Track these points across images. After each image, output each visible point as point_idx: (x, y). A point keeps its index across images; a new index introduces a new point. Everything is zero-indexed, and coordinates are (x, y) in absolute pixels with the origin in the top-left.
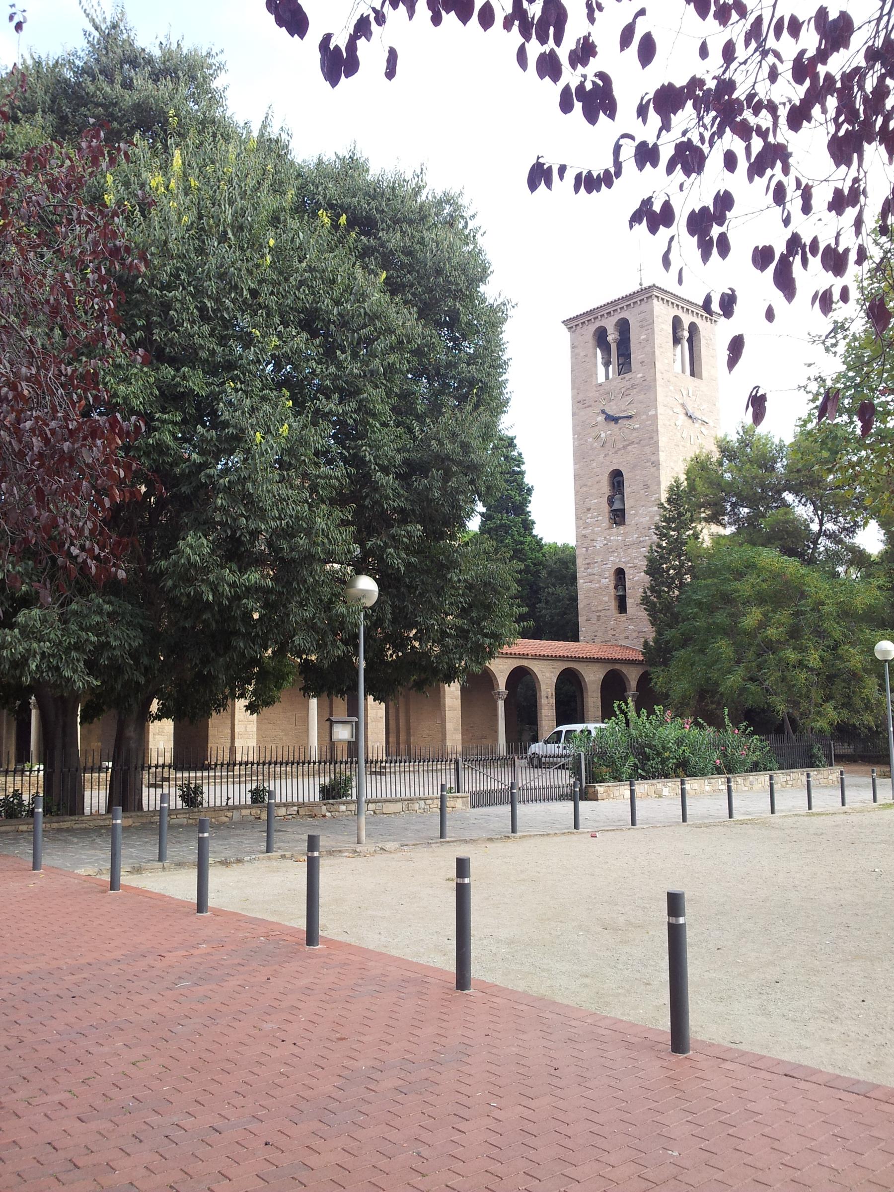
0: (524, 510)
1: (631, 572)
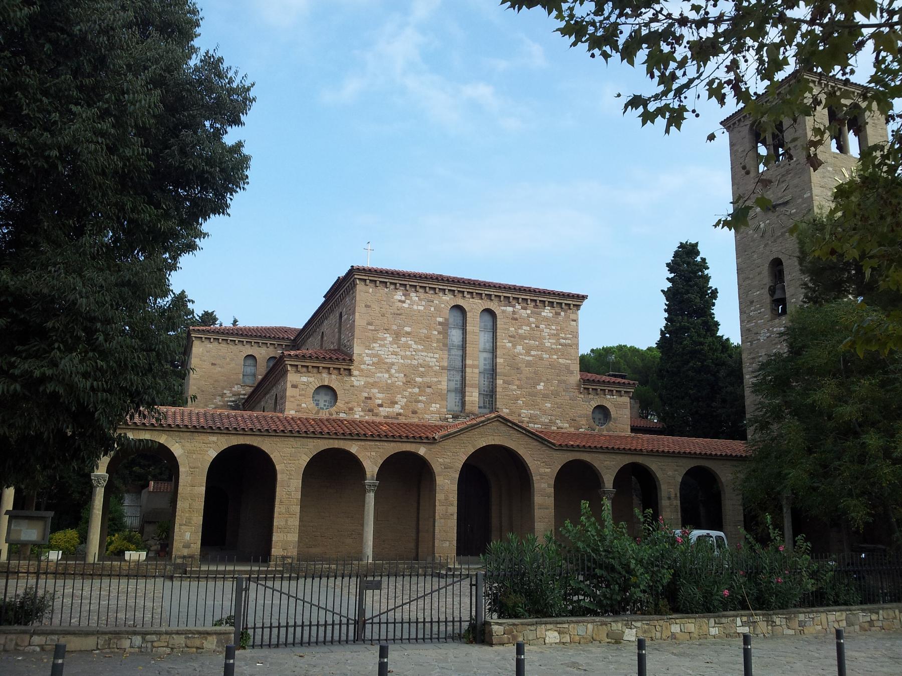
0: (705, 312)
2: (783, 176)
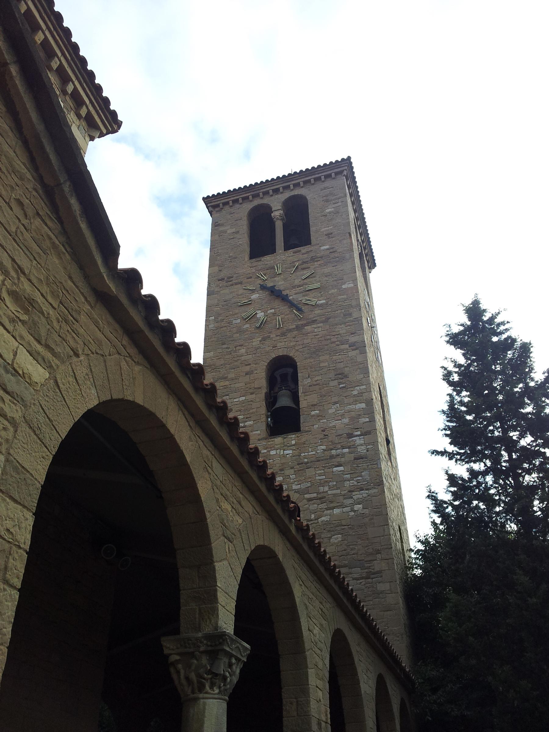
1: (314, 507)
2: (304, 263)
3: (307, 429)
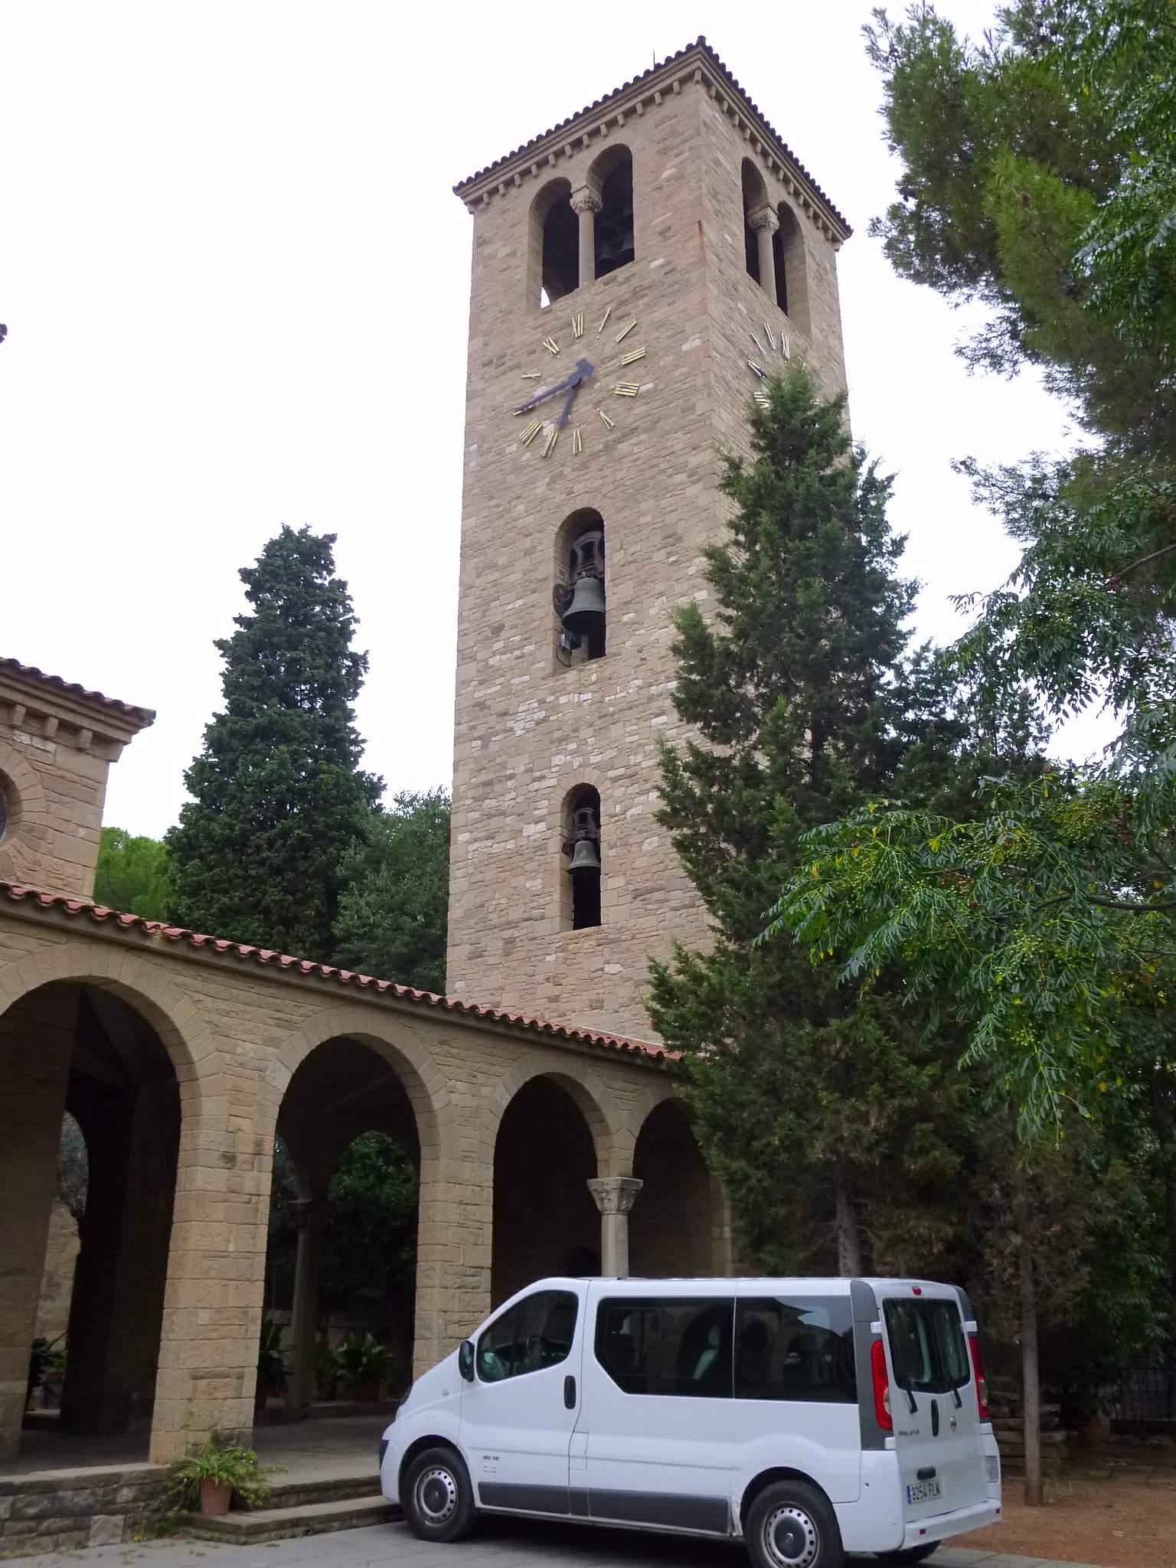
1: (619, 792)
2: (621, 304)
3: (614, 650)
